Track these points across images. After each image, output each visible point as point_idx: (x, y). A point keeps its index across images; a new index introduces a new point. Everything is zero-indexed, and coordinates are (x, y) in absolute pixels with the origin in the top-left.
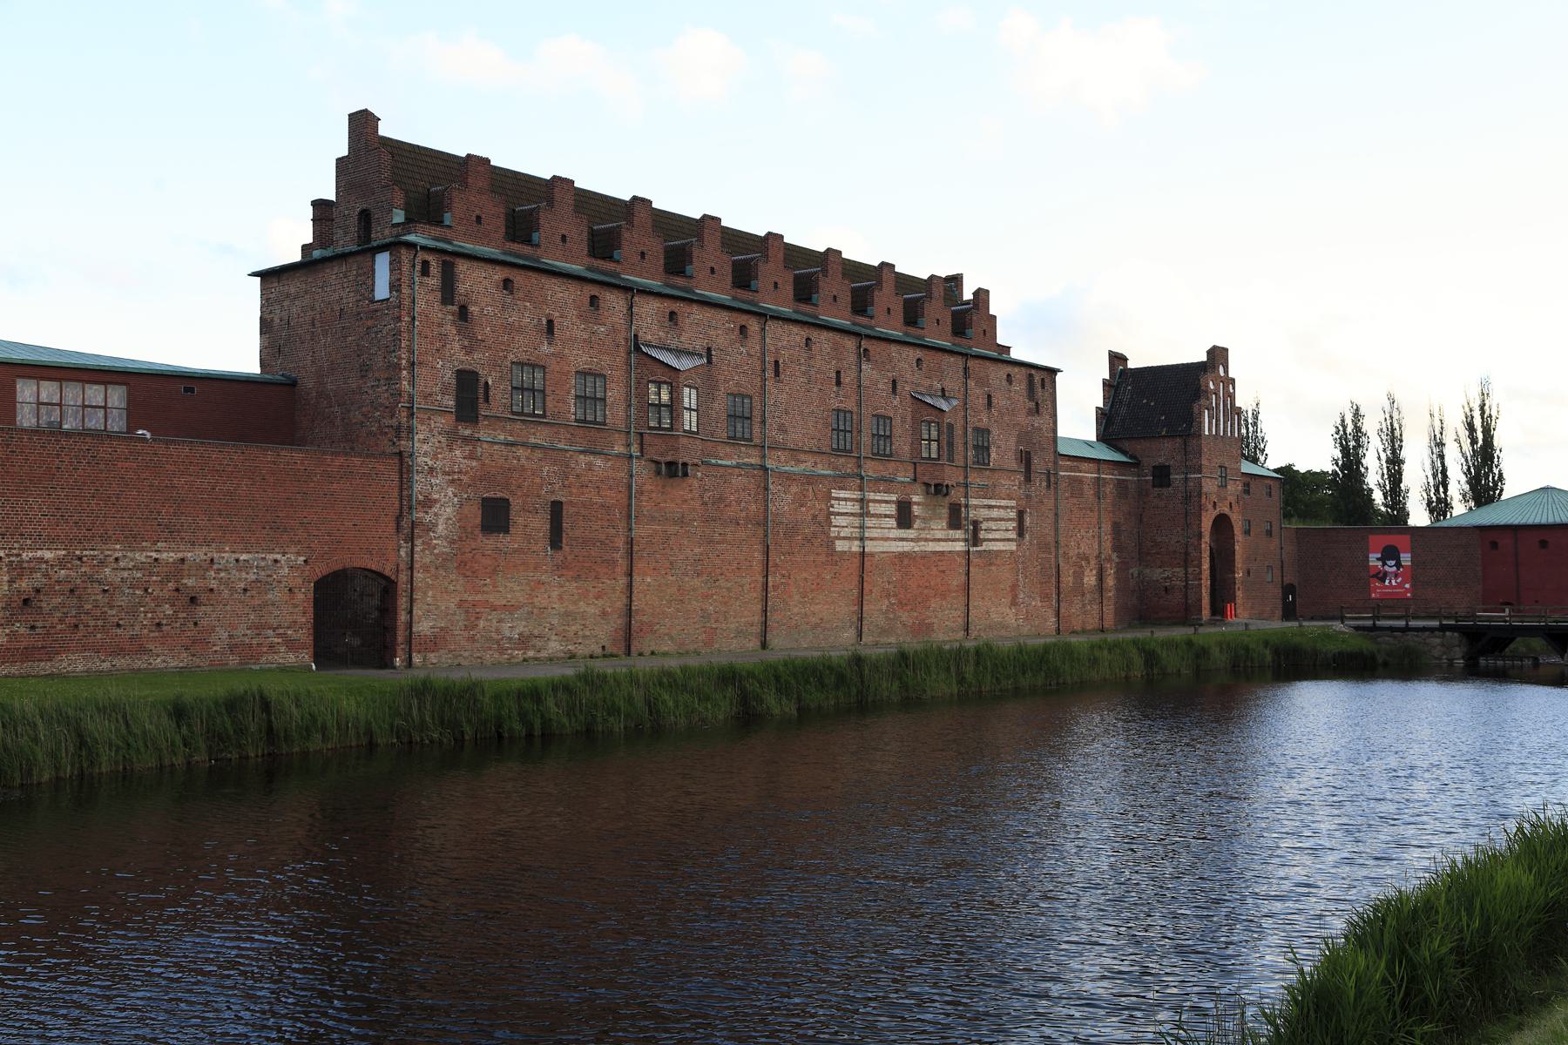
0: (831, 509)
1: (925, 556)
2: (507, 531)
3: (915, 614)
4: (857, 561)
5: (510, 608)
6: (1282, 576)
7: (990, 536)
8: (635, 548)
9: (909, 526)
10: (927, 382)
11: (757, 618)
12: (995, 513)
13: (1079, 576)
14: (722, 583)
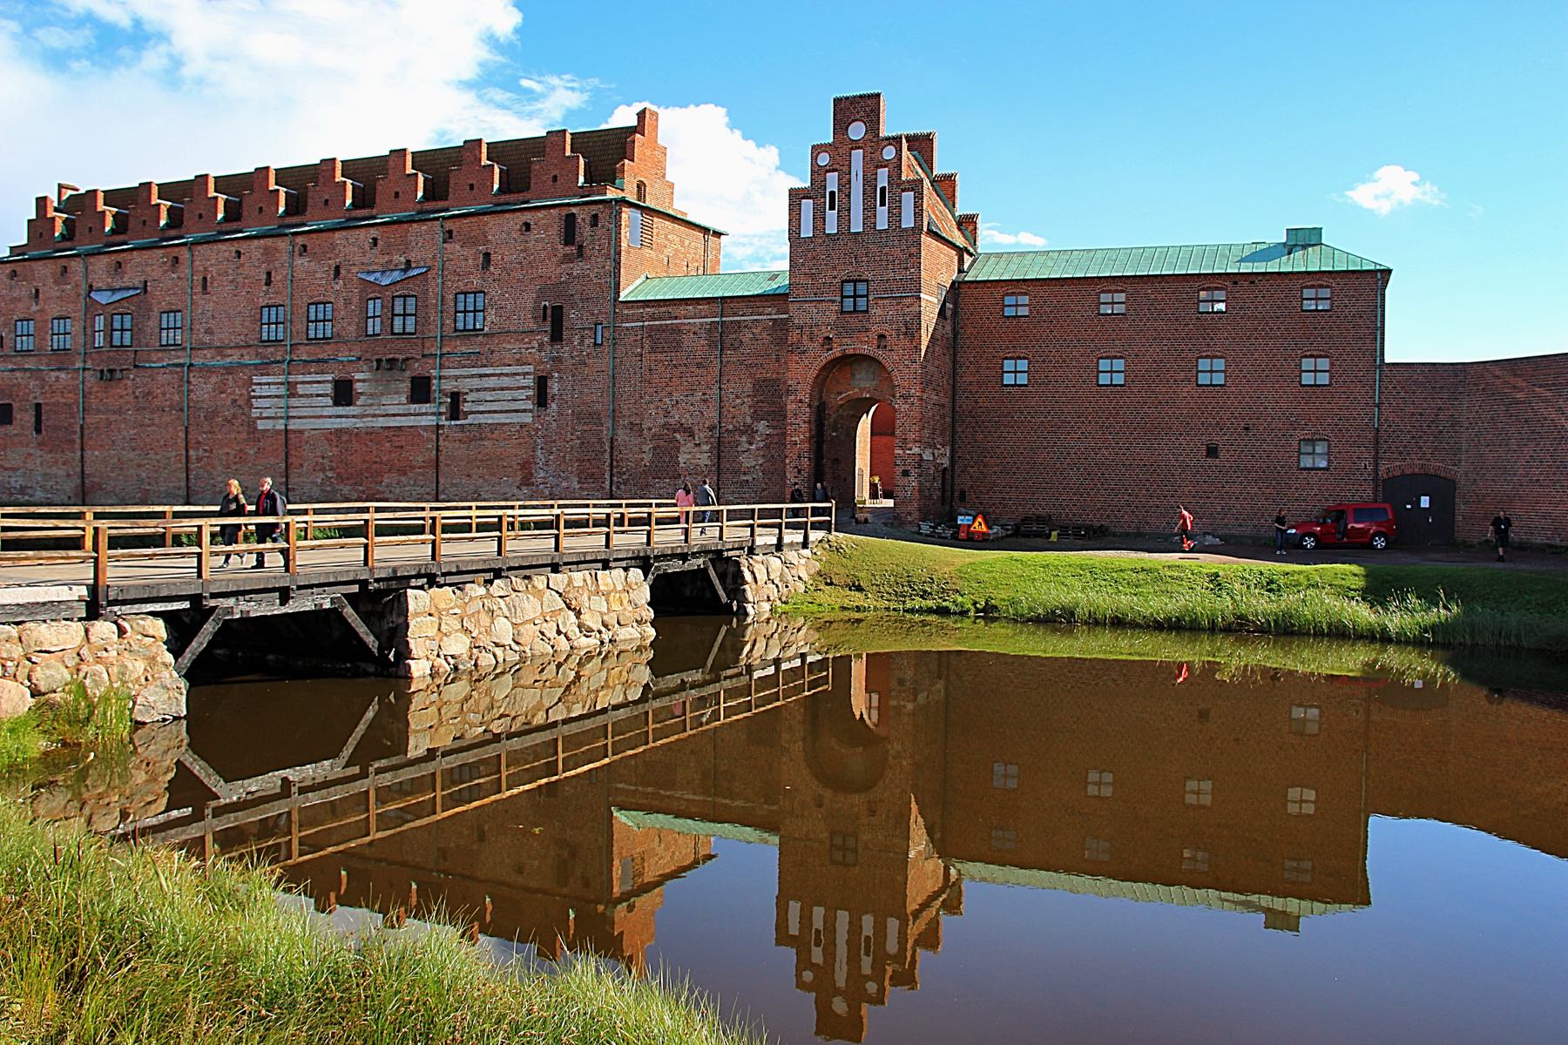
0: (252, 394)
1: (370, 432)
2: (11, 423)
3: (361, 488)
4: (283, 434)
5: (14, 469)
6: (1376, 459)
7: (482, 408)
8: (86, 432)
9: (349, 404)
10: (387, 258)
11: (183, 484)
12: (492, 382)
13: (666, 449)
14: (152, 455)
